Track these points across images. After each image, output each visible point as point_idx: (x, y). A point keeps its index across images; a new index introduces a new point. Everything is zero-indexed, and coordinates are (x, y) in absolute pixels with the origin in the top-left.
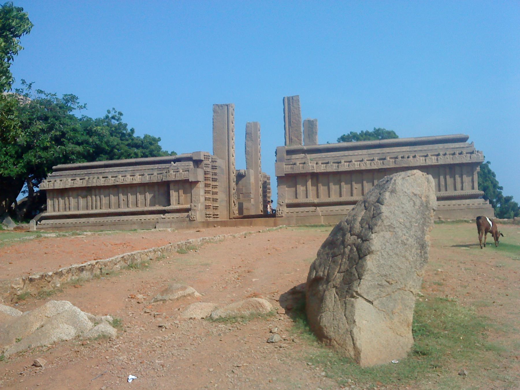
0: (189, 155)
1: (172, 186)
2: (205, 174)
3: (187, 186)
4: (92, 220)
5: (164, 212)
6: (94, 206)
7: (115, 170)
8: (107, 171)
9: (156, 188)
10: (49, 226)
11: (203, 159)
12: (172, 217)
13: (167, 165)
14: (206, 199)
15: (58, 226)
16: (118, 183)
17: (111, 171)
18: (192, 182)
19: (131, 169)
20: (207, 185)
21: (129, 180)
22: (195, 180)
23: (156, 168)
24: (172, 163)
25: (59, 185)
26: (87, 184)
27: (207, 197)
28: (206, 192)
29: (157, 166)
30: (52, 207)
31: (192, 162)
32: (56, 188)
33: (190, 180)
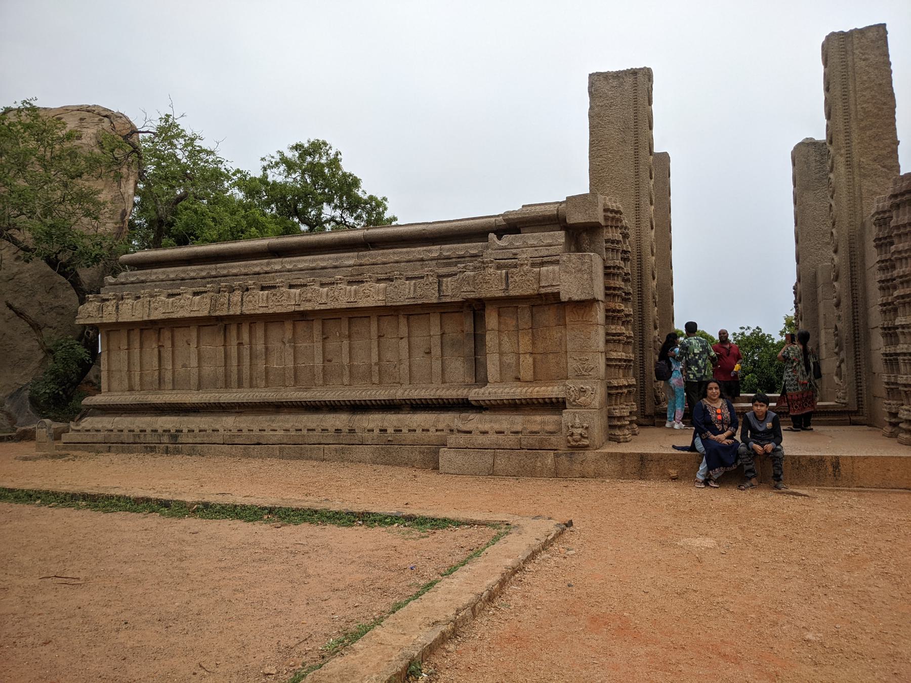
0: (553, 210)
1: (492, 320)
2: (607, 275)
3: (548, 316)
4: (229, 422)
5: (463, 406)
6: (234, 377)
7: (300, 266)
8: (278, 267)
9: (435, 320)
10: (100, 437)
11: (602, 221)
12: (497, 427)
13: (473, 247)
14: (610, 364)
15: (125, 437)
16: (308, 306)
17: (289, 267)
18: (570, 302)
19: (351, 262)
20: (612, 316)
21: (344, 296)
22: (583, 297)
23: (435, 255)
24: (492, 236)
25: (132, 311)
26: (213, 307)
27: (614, 355)
28: (611, 339)
29: (435, 250)
30: (119, 375)
31: (562, 233)
32: (120, 320)
33: (564, 297)
